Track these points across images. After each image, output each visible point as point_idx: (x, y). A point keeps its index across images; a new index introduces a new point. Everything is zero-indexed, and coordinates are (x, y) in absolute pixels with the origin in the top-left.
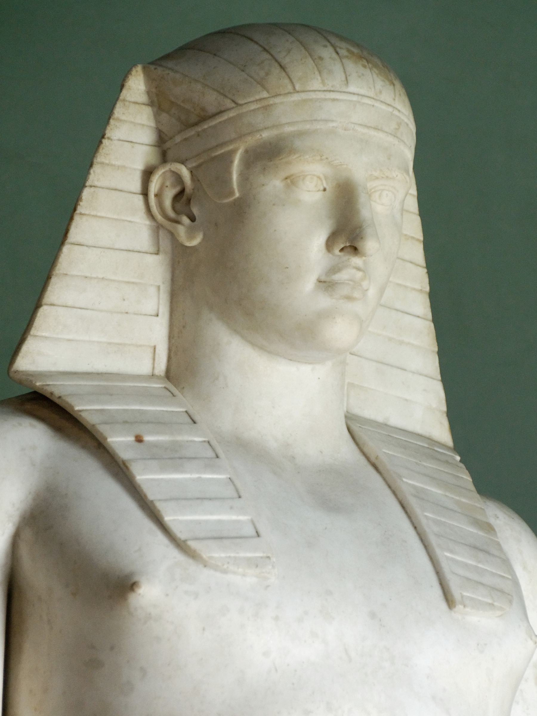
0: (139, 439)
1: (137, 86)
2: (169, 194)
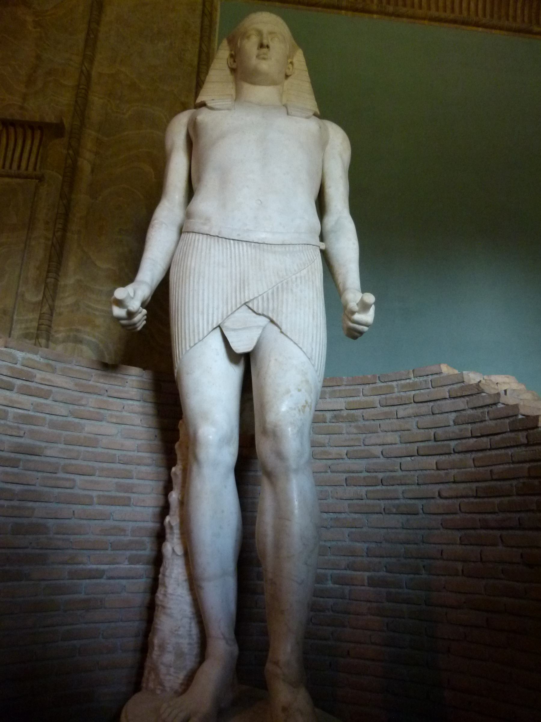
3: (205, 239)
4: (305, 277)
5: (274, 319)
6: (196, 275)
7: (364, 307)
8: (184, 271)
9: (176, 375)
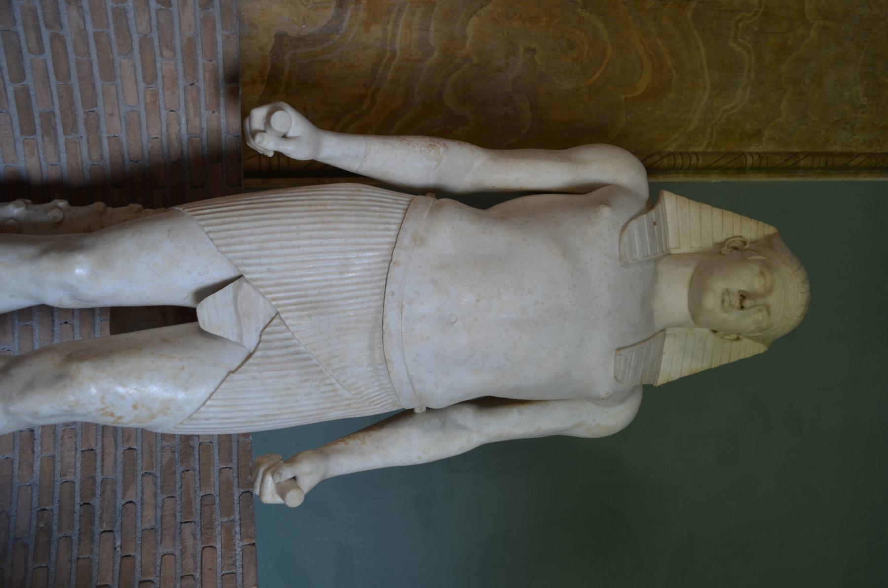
0: (655, 224)
1: (770, 230)
2: (736, 245)
3: (389, 240)
4: (336, 396)
5: (251, 361)
6: (323, 233)
7: (282, 491)
8: (335, 212)
9: (177, 208)
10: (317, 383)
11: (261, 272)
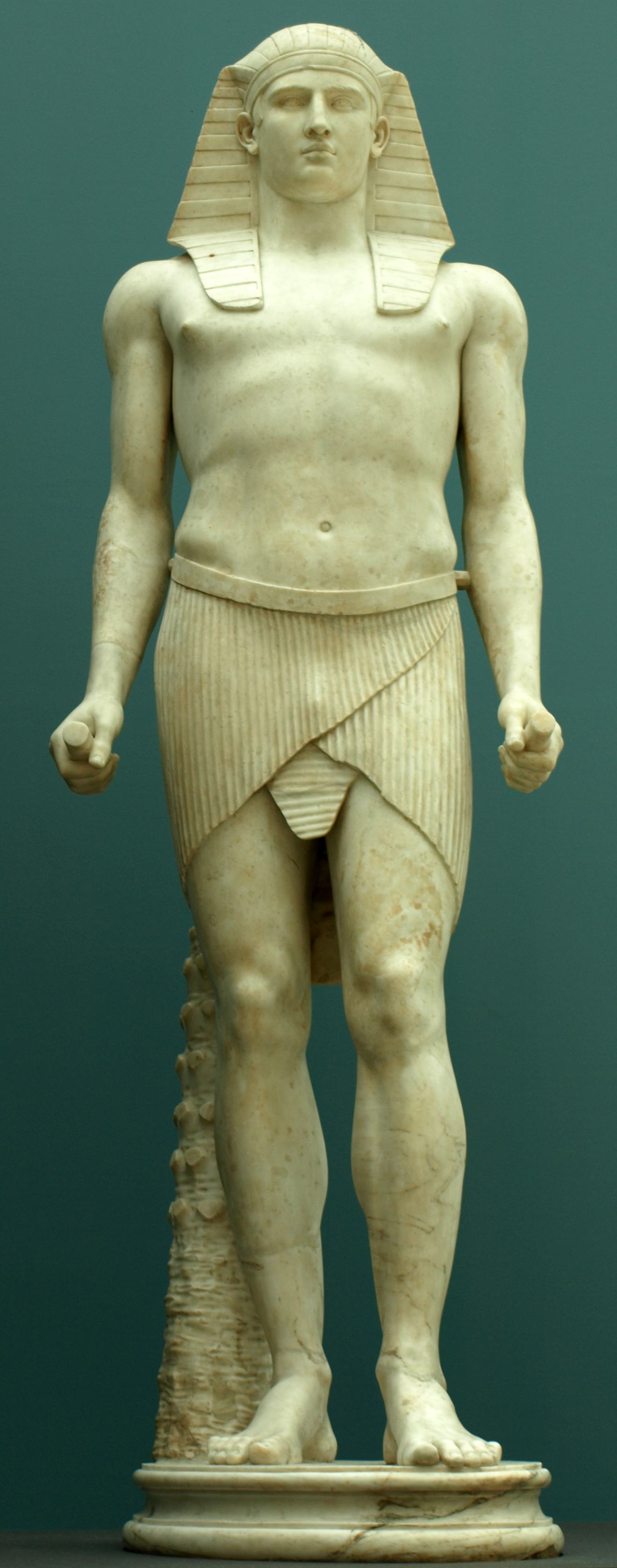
10: (403, 698)
11: (260, 762)
